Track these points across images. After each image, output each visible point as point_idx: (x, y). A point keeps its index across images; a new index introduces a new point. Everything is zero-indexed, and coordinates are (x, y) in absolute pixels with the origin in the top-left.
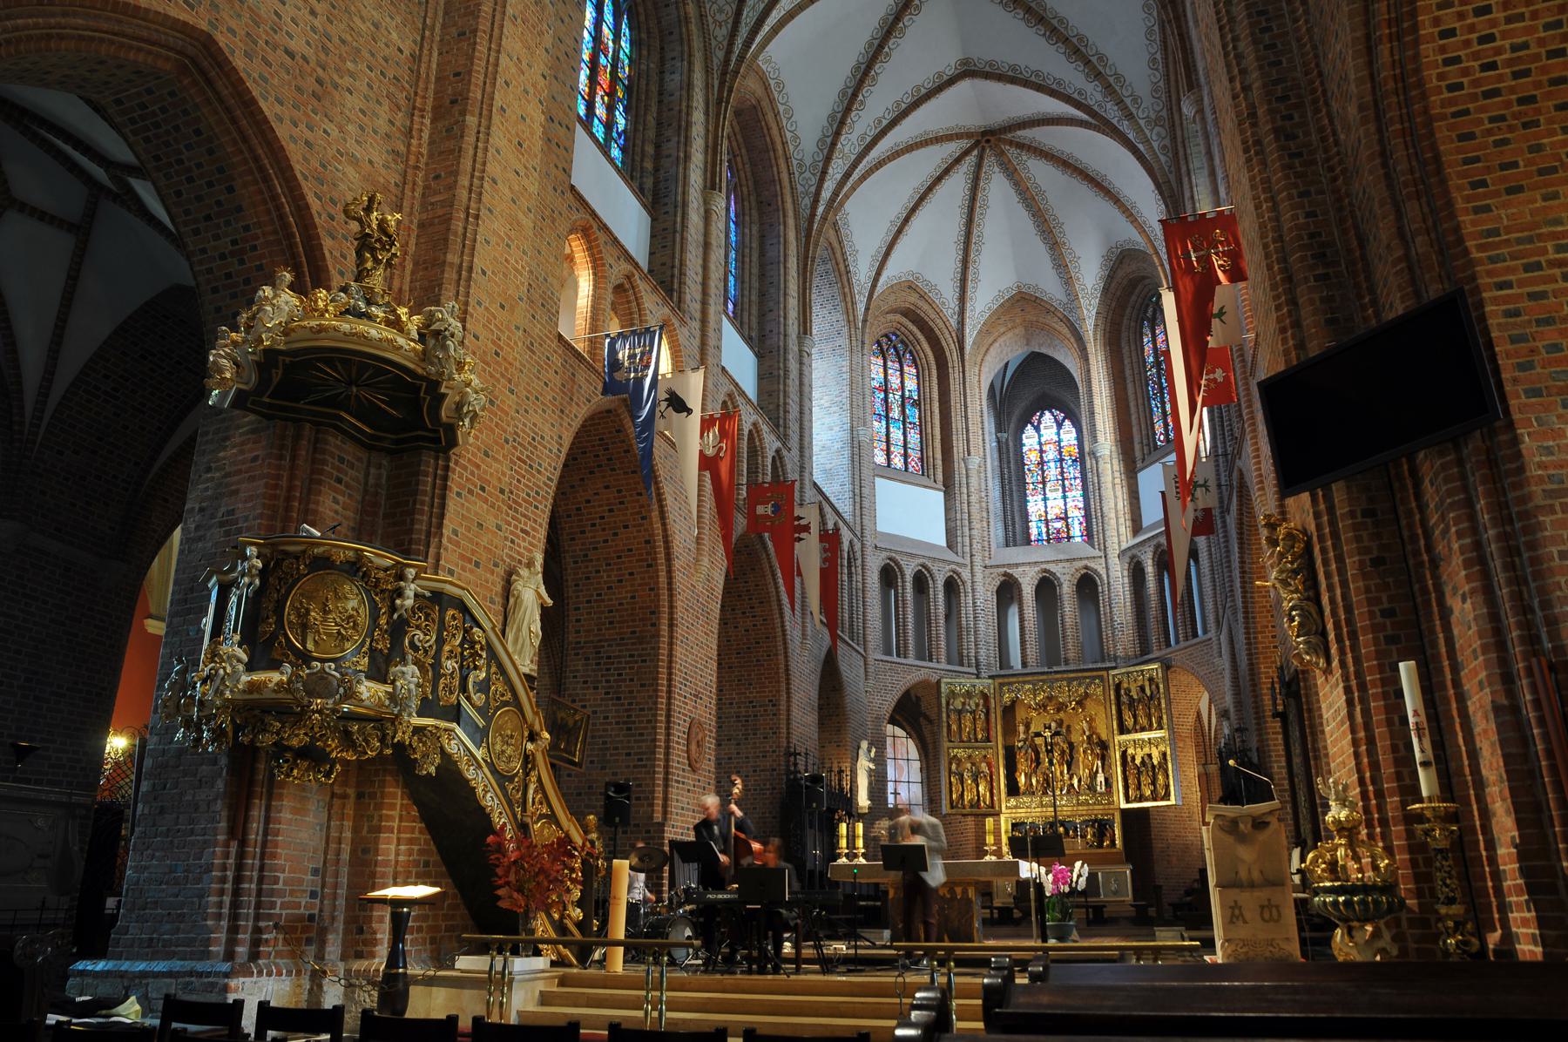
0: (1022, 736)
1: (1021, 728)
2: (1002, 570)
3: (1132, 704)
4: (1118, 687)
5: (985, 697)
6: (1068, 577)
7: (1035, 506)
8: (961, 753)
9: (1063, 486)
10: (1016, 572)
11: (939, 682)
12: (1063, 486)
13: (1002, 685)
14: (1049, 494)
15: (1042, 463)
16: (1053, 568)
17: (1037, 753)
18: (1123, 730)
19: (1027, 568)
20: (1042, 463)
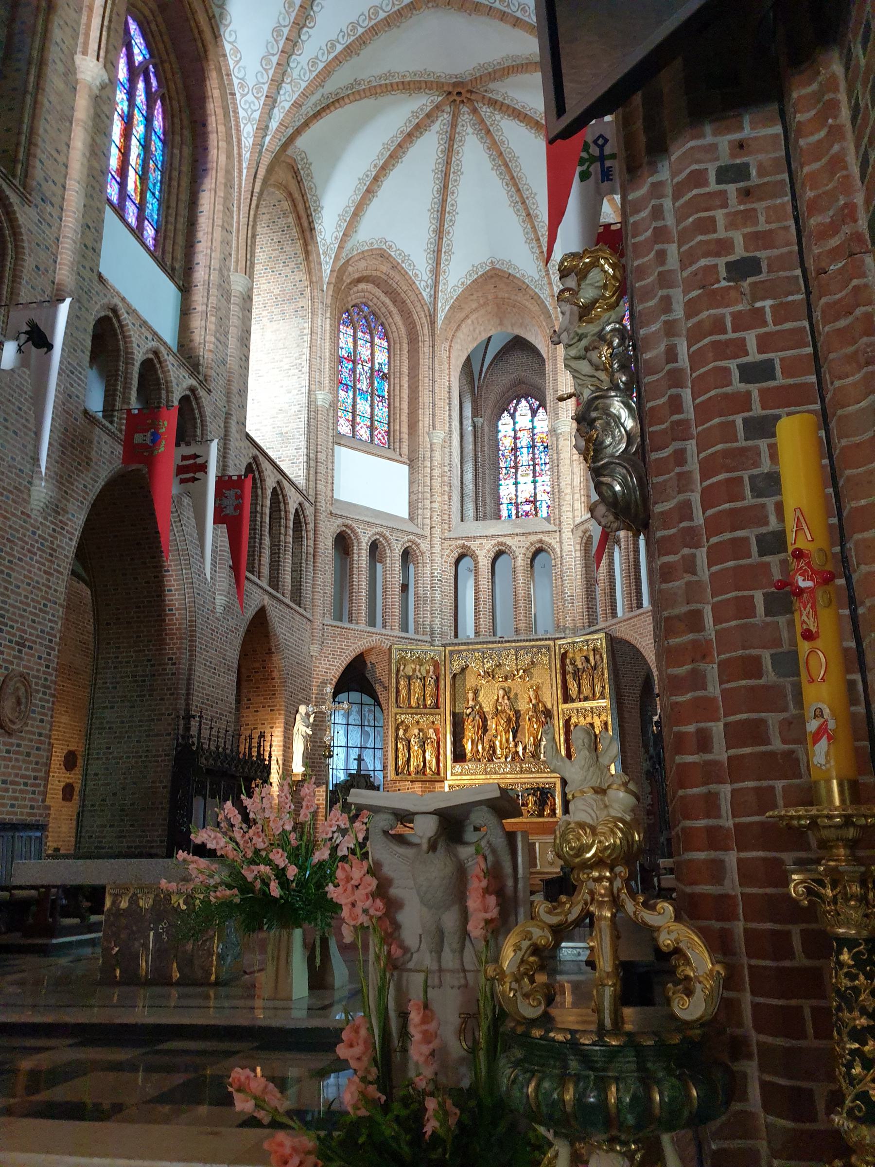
0: (471, 703)
1: (471, 695)
2: (460, 542)
3: (577, 674)
4: (564, 656)
5: (436, 665)
6: (523, 551)
7: (506, 490)
8: (408, 719)
9: (534, 471)
10: (473, 545)
11: (390, 649)
12: (534, 471)
13: (451, 652)
14: (520, 479)
15: (515, 449)
16: (509, 541)
17: (485, 720)
18: (567, 699)
19: (484, 541)
20: (515, 449)
